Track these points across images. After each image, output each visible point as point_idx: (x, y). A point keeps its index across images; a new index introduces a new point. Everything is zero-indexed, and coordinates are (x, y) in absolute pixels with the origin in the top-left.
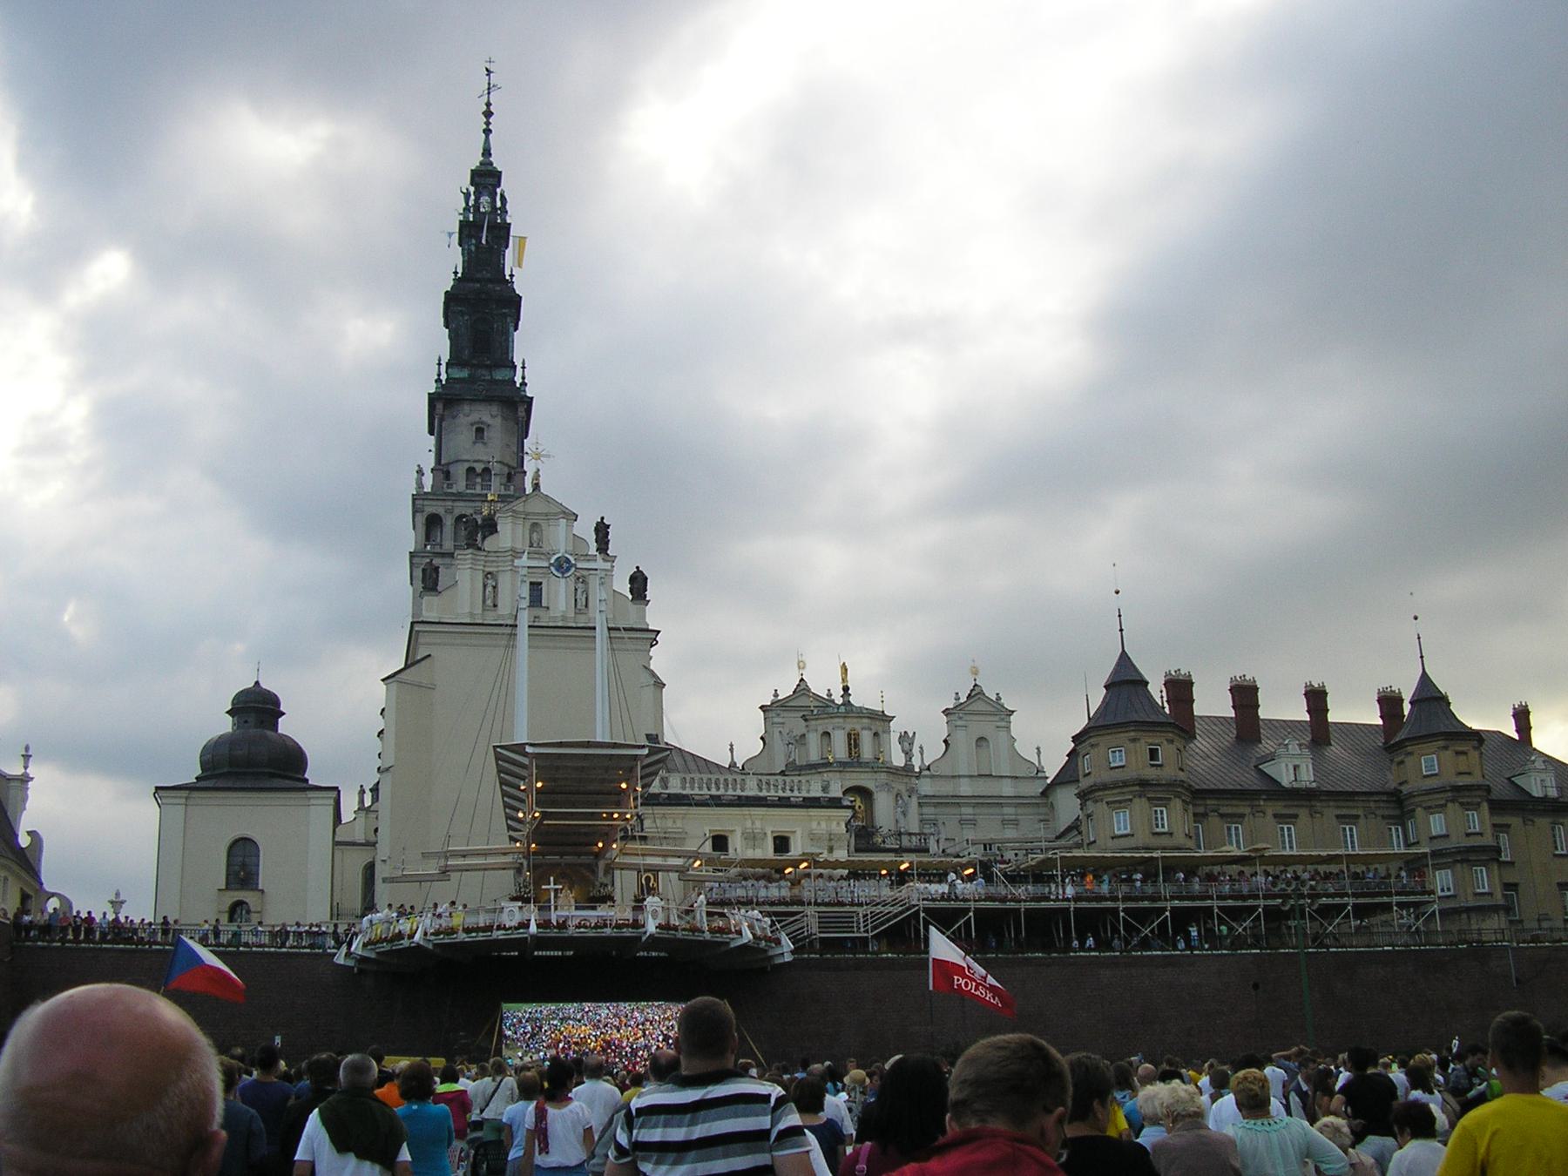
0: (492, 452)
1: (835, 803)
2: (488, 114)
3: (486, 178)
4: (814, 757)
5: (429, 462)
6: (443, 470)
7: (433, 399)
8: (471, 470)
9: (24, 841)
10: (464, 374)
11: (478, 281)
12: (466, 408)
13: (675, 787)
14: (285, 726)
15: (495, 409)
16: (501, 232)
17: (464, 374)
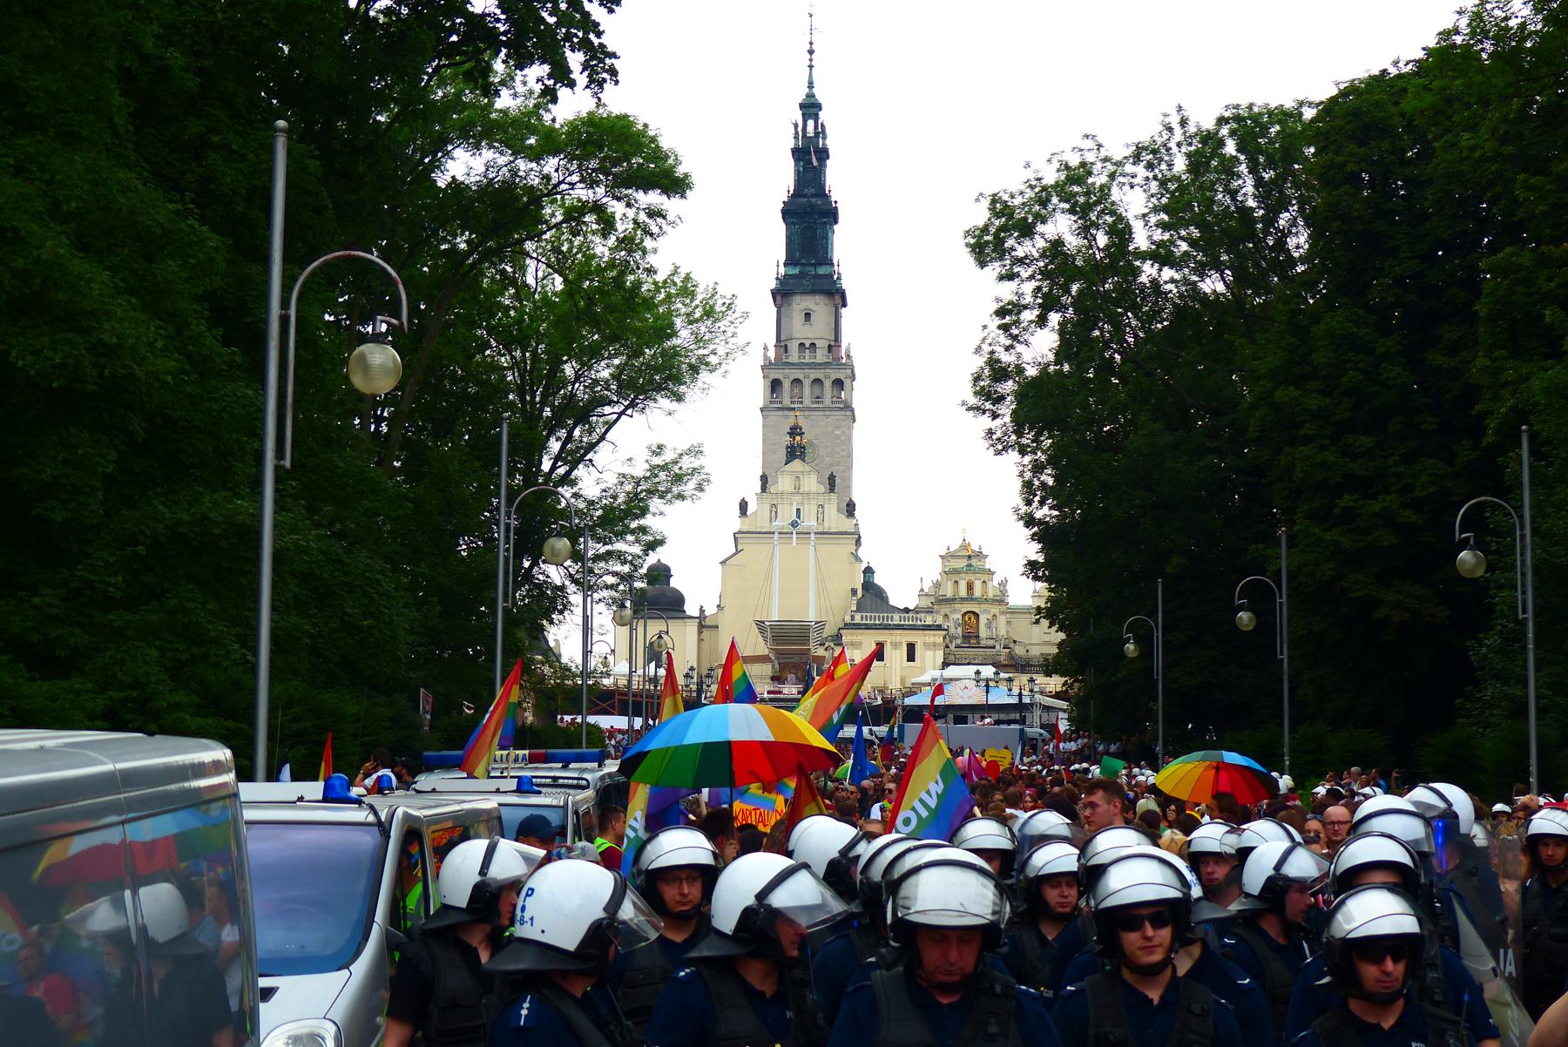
0: (818, 330)
1: (939, 628)
2: (811, 52)
3: (810, 108)
4: (950, 595)
5: (772, 341)
6: (782, 345)
7: (774, 293)
8: (802, 345)
9: (552, 644)
10: (796, 271)
11: (805, 196)
12: (797, 298)
13: (858, 619)
14: (674, 583)
15: (818, 298)
16: (823, 154)
17: (796, 271)
